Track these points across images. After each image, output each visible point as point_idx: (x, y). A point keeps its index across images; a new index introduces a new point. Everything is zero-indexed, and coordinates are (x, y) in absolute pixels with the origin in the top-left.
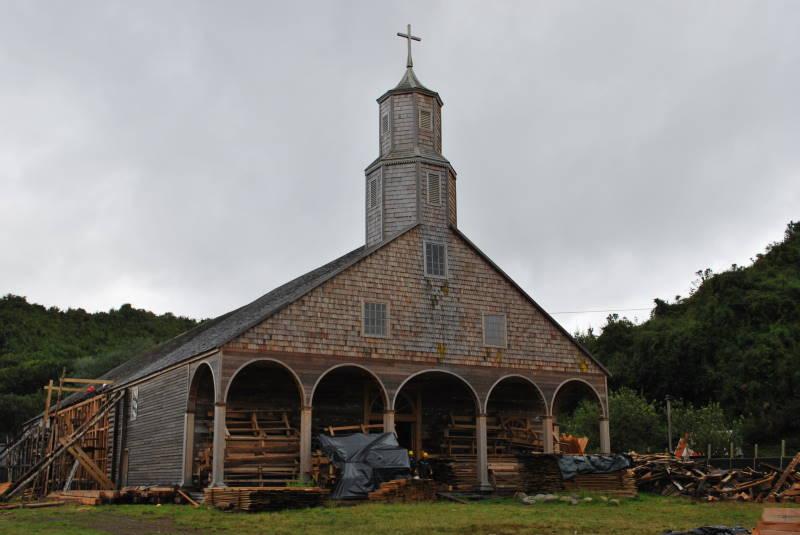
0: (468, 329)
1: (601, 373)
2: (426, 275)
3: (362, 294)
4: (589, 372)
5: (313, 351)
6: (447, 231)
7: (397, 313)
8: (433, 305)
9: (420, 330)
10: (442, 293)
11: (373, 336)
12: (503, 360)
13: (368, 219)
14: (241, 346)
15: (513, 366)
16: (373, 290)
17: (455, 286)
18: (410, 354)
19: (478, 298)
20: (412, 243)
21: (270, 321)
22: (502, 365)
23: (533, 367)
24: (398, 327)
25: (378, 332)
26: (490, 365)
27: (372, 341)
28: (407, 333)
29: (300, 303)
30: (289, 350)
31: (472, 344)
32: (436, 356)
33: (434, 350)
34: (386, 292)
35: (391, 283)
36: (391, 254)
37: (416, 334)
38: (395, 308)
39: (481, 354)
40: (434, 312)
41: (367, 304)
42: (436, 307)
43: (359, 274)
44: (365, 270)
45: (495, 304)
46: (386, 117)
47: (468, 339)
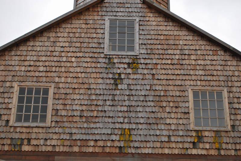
0: (168, 109)
2: (106, 51)
3: (16, 79)
6: (140, 6)
7: (63, 96)
8: (116, 85)
9: (95, 114)
10: (129, 71)
11: (26, 124)
12: (224, 146)
16: (32, 74)
17: (148, 61)
18: (79, 143)
19: (182, 72)
20: (91, 22)
22: (223, 153)
24: (64, 113)
25: (35, 119)
26: (204, 152)
27: (24, 130)
28: (78, 119)
31: (173, 127)
32: (117, 144)
33: (114, 137)
34: (49, 74)
35: (56, 64)
36: (59, 35)
37: (88, 120)
38: (62, 91)
39: (189, 140)
40: (118, 92)
41: (22, 91)
42: (120, 87)
43: (17, 58)
44: (25, 53)
45: (209, 78)
47: (168, 121)
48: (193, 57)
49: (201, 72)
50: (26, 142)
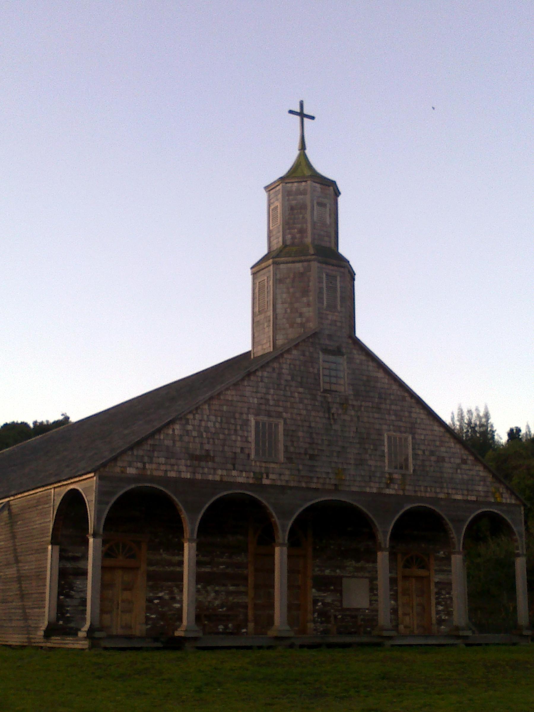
1: (518, 502)
4: (504, 501)
5: (199, 477)
13: (255, 324)
14: (118, 470)
15: (419, 494)
21: (150, 442)
22: (407, 493)
23: (442, 496)
24: (292, 449)
29: (184, 422)
30: (172, 474)
41: (257, 423)
46: (277, 207)
47: (370, 463)
48: (388, 401)
49: (393, 418)
50: (265, 476)
